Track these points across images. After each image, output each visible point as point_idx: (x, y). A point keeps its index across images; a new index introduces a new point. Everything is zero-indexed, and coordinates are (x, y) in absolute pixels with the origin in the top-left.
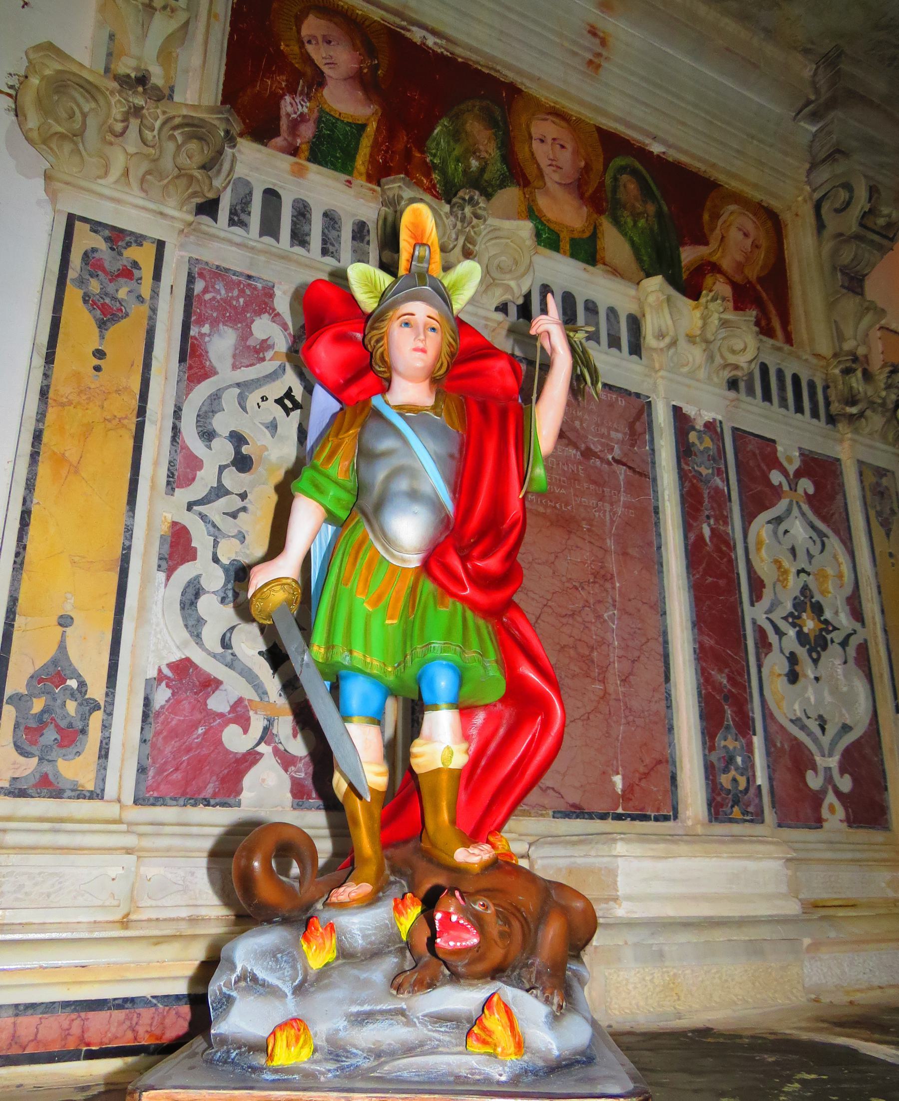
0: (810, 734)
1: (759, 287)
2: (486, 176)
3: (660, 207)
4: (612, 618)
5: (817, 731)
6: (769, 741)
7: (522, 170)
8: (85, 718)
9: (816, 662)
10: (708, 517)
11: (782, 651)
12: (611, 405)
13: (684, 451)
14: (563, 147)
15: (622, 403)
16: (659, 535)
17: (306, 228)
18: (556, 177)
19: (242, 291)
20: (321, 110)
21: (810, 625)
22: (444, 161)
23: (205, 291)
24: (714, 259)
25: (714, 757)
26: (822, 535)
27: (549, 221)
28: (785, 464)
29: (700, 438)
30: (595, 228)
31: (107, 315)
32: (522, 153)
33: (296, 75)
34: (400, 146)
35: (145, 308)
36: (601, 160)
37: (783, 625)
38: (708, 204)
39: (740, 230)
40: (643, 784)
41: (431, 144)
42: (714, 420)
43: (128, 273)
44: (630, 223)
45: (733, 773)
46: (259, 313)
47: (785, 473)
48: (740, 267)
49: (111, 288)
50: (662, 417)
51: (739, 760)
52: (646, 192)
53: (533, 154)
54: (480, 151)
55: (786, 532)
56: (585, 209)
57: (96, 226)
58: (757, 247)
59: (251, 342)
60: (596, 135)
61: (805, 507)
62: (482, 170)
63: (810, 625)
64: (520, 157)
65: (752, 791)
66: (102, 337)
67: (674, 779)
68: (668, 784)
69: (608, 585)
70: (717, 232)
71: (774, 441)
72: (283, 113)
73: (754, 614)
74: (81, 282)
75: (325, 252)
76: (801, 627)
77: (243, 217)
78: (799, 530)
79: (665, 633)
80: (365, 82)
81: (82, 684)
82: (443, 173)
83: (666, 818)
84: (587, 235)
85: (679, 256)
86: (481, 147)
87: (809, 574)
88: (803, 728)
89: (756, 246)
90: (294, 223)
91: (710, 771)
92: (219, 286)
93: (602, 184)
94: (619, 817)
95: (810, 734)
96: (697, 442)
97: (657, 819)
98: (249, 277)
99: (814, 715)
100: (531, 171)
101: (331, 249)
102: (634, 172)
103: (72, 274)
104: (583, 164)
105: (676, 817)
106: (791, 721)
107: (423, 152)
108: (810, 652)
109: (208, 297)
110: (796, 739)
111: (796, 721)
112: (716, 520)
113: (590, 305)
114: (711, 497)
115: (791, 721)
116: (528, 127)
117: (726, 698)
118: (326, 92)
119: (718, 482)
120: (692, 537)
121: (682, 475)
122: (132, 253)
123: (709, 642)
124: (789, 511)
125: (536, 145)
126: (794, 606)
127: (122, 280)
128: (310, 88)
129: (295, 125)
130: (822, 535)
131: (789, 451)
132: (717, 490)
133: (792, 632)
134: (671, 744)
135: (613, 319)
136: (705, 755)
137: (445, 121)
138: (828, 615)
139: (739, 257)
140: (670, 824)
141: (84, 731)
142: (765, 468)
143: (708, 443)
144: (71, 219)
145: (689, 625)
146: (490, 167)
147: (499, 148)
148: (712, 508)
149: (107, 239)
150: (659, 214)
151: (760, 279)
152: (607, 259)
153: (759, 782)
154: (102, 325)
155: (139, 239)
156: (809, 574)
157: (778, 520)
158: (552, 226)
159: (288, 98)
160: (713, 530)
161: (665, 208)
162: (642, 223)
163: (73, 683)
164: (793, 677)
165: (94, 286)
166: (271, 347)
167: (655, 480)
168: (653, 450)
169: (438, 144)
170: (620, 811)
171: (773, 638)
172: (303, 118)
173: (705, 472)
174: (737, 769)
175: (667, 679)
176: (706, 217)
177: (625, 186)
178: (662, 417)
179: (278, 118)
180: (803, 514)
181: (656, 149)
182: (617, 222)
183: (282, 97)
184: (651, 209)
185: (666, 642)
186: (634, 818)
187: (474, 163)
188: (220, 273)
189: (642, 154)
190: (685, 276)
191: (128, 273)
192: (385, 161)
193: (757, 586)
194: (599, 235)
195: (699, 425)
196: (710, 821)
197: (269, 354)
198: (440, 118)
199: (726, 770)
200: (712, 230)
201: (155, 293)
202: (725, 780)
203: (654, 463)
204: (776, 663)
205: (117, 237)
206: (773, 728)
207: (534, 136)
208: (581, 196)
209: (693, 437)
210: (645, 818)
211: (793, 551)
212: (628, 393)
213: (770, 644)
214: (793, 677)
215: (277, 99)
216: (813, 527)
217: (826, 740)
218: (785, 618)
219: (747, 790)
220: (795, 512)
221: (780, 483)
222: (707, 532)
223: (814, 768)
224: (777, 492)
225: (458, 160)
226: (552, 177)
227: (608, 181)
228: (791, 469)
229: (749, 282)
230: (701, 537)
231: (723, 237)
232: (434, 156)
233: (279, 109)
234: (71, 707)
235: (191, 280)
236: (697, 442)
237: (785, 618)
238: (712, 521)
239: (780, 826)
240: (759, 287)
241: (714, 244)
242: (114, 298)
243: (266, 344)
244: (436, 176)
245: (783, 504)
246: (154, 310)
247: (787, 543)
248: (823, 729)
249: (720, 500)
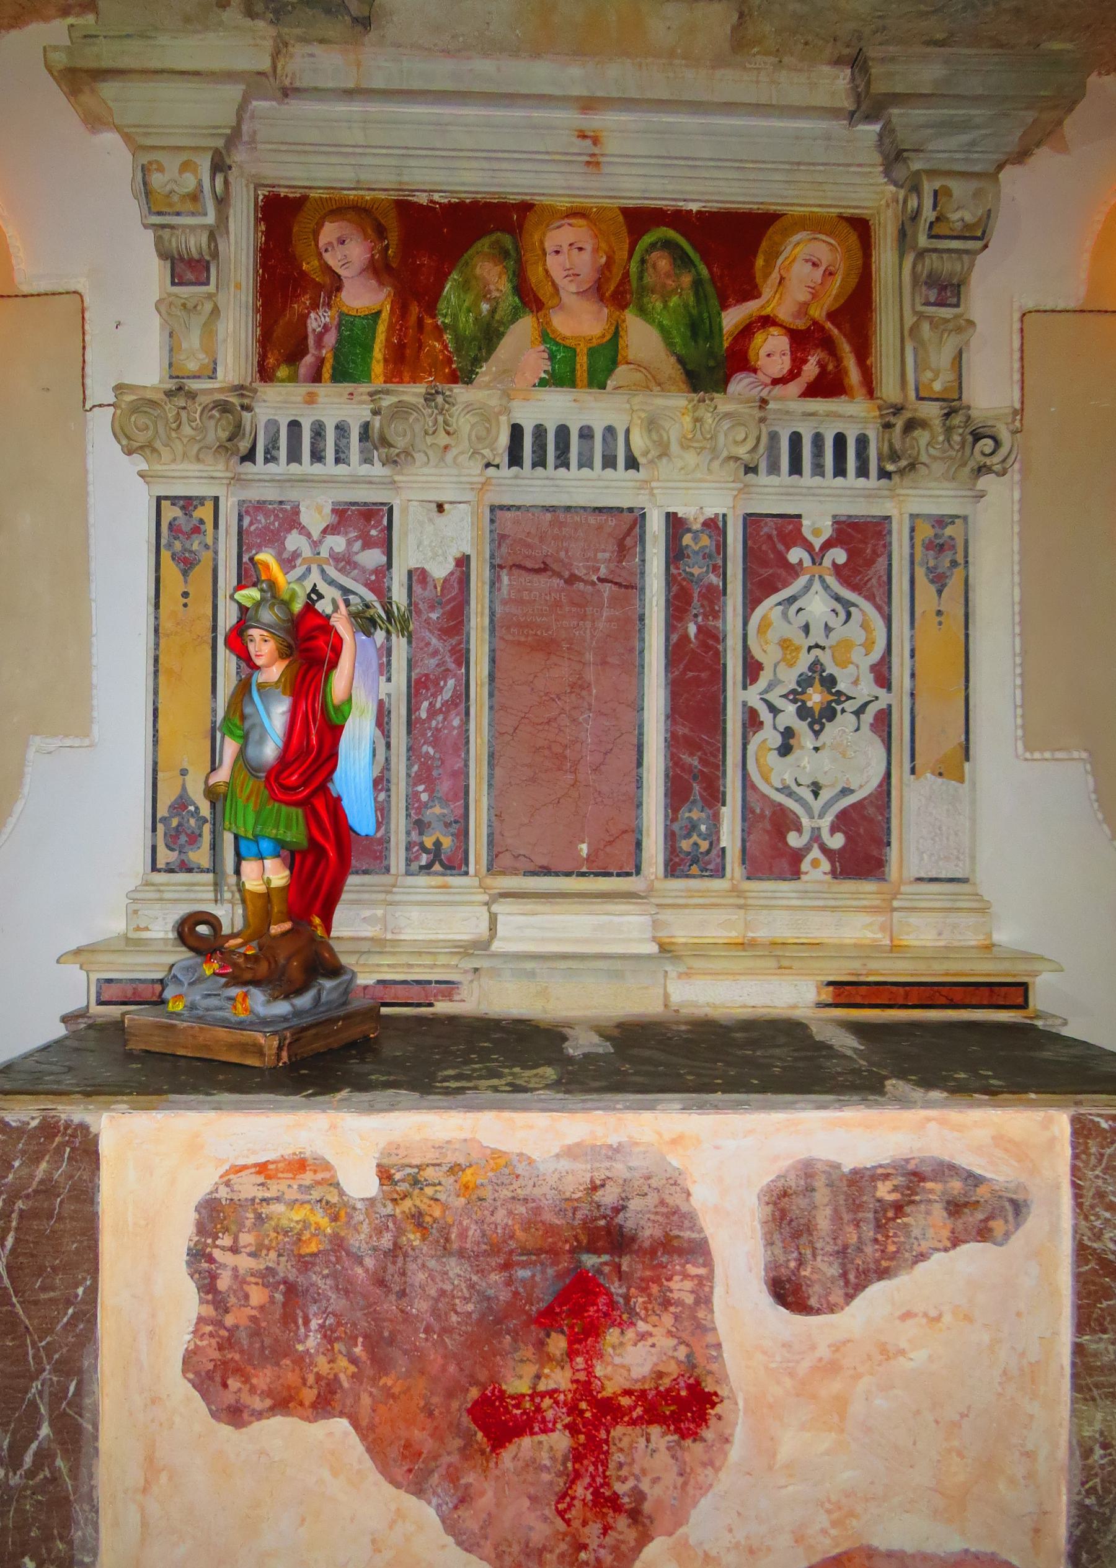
0: (799, 800)
1: (829, 325)
2: (497, 317)
3: (698, 274)
4: (586, 721)
5: (808, 796)
6: (746, 808)
7: (535, 295)
8: (201, 828)
9: (817, 734)
10: (696, 616)
11: (775, 728)
12: (600, 528)
13: (675, 554)
14: (580, 249)
15: (612, 522)
16: (643, 640)
17: (321, 445)
18: (573, 288)
19: (276, 516)
20: (341, 315)
21: (816, 698)
22: (455, 317)
23: (251, 523)
24: (768, 311)
25: (676, 827)
26: (847, 604)
27: (564, 338)
28: (810, 538)
29: (696, 539)
30: (617, 328)
31: (187, 564)
32: (535, 275)
33: (319, 287)
34: (413, 319)
35: (210, 553)
36: (626, 246)
37: (779, 703)
38: (764, 244)
39: (807, 261)
40: (608, 849)
41: (442, 306)
42: (717, 515)
43: (196, 530)
44: (659, 305)
45: (695, 838)
46: (289, 531)
47: (808, 547)
48: (803, 309)
49: (188, 546)
50: (656, 526)
51: (703, 828)
52: (682, 260)
53: (547, 271)
54: (489, 291)
55: (800, 609)
56: (606, 310)
57: (174, 500)
58: (831, 274)
59: (285, 556)
60: (621, 218)
61: (831, 580)
62: (493, 311)
63: (816, 698)
64: (533, 280)
65: (714, 852)
66: (186, 582)
67: (639, 844)
68: (632, 848)
69: (584, 693)
70: (775, 276)
71: (799, 516)
72: (310, 330)
73: (737, 698)
74: (169, 545)
75: (338, 461)
76: (804, 702)
77: (274, 453)
78: (817, 606)
79: (641, 726)
80: (378, 269)
81: (197, 808)
82: (453, 327)
83: (628, 874)
84: (608, 337)
85: (720, 323)
86: (492, 287)
87: (823, 648)
88: (791, 794)
89: (829, 274)
90: (312, 444)
91: (671, 837)
92: (261, 517)
93: (626, 275)
94: (583, 874)
95: (799, 800)
96: (691, 543)
97: (619, 875)
98: (281, 503)
99: (806, 780)
100: (545, 293)
101: (342, 456)
102: (667, 245)
103: (163, 541)
104: (603, 260)
105: (638, 872)
106: (777, 790)
107: (434, 316)
108: (811, 726)
109: (252, 528)
110: (780, 804)
111: (785, 790)
112: (706, 616)
113: (586, 431)
114: (702, 596)
115: (777, 790)
116: (542, 242)
117: (695, 778)
118: (344, 294)
119: (714, 579)
120: (675, 638)
121: (670, 580)
122: (199, 513)
123: (681, 731)
124: (807, 588)
125: (551, 261)
126: (799, 683)
127: (194, 536)
128: (330, 298)
129: (320, 338)
130: (847, 604)
131: (818, 524)
132: (710, 588)
133: (791, 708)
134: (639, 817)
135: (609, 439)
136: (666, 826)
137: (455, 275)
138: (841, 686)
139: (803, 296)
140: (633, 879)
141: (200, 835)
142: (781, 547)
143: (705, 541)
144: (159, 499)
145: (662, 718)
146: (501, 305)
147: (511, 281)
148: (702, 606)
149: (183, 508)
150: (697, 284)
151: (831, 316)
152: (631, 357)
153: (723, 844)
154: (185, 573)
155: (201, 500)
156: (823, 648)
157: (792, 600)
158: (567, 343)
159: (312, 315)
160: (700, 629)
161: (704, 272)
162: (674, 301)
163: (192, 808)
164: (785, 750)
165: (178, 546)
166: (300, 555)
167: (643, 589)
168: (643, 561)
169: (449, 301)
170: (584, 869)
171: (765, 715)
172: (326, 328)
173: (696, 571)
174: (699, 835)
175: (640, 764)
176: (760, 262)
177: (654, 266)
178: (656, 526)
179: (306, 337)
180: (826, 587)
181: (694, 207)
182: (642, 311)
183: (307, 316)
184: (687, 279)
185: (641, 734)
186: (597, 875)
187: (485, 307)
188: (260, 506)
189: (677, 219)
190: (726, 345)
191: (196, 530)
192: (400, 340)
193: (752, 670)
194: (622, 333)
195: (697, 526)
196: (666, 877)
197: (299, 561)
198: (450, 273)
199: (688, 836)
200: (767, 276)
201: (216, 539)
202: (685, 845)
203: (643, 573)
204: (769, 736)
205: (188, 503)
206: (752, 797)
207: (548, 250)
208: (602, 298)
209: (687, 539)
210: (609, 875)
211: (806, 629)
212: (620, 510)
213: (762, 723)
214: (785, 750)
215: (304, 318)
216: (838, 598)
217: (817, 805)
218: (785, 696)
219: (708, 852)
220: (817, 585)
221: (801, 561)
222: (692, 629)
223: (799, 829)
224: (794, 571)
225: (469, 311)
226: (568, 288)
227: (634, 267)
228: (817, 543)
229: (815, 323)
230: (685, 637)
231: (782, 279)
232: (445, 316)
233: (306, 327)
234: (192, 822)
235: (240, 518)
236: (691, 543)
237: (785, 696)
238: (700, 619)
239: (748, 878)
240: (829, 325)
241: (767, 292)
242: (191, 552)
243: (296, 555)
244: (447, 337)
245: (802, 580)
246: (216, 553)
247: (801, 619)
248: (816, 794)
249: (714, 597)
